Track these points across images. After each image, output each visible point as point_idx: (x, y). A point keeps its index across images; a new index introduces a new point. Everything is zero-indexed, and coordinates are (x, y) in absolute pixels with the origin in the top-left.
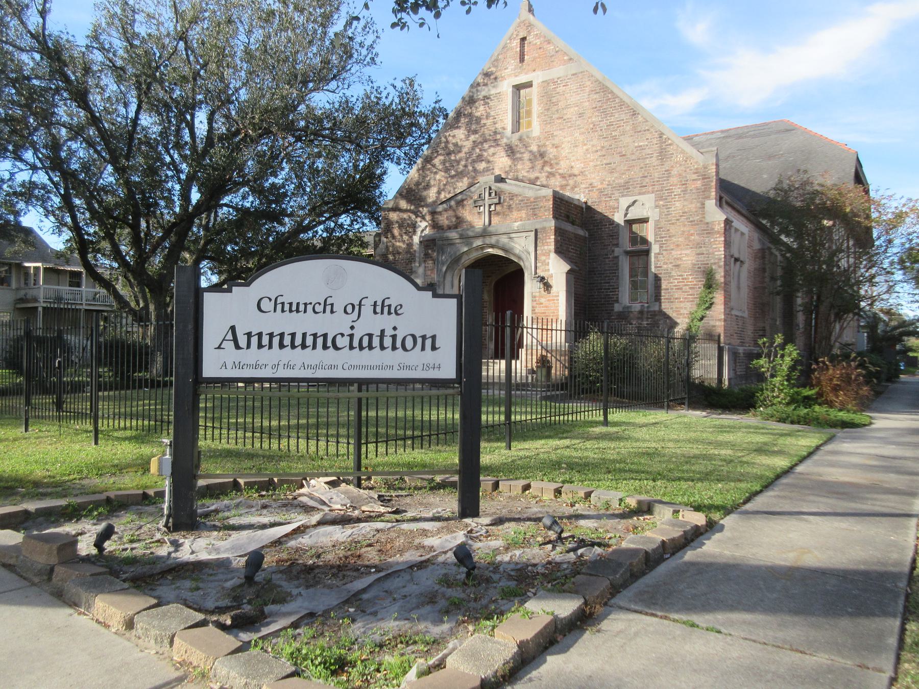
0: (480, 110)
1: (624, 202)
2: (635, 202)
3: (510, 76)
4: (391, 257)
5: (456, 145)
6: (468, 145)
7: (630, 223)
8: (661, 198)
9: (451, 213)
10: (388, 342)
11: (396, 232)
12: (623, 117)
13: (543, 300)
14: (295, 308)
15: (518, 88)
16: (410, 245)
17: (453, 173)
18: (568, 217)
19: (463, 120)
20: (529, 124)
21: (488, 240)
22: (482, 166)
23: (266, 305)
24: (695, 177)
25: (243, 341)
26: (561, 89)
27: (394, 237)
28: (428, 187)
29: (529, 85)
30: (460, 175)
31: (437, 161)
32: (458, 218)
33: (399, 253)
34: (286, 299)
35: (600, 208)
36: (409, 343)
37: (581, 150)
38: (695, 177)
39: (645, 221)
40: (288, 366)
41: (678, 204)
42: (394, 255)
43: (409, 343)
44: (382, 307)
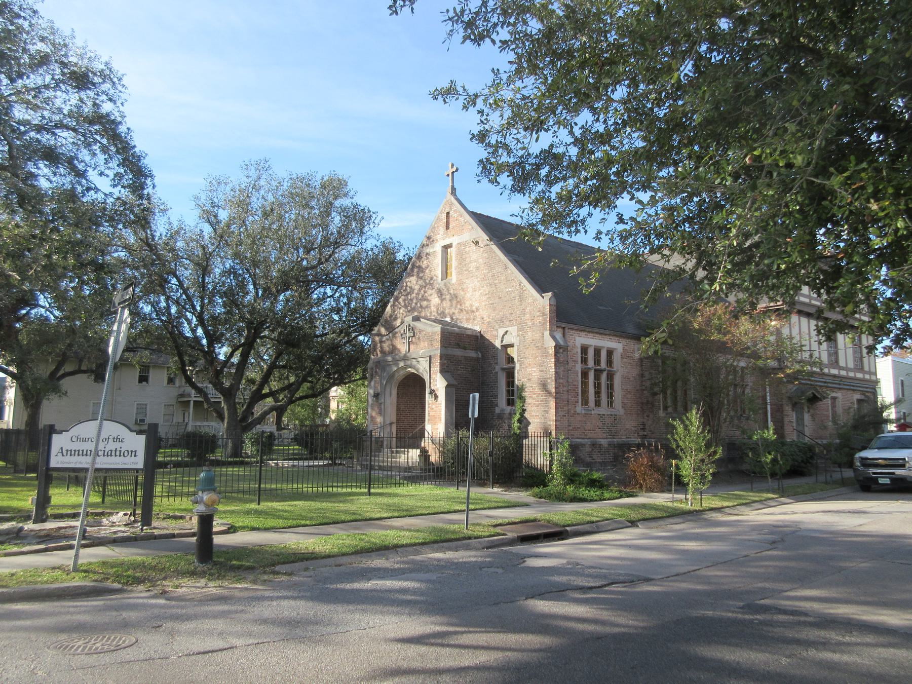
0: (424, 264)
1: (501, 332)
2: (506, 332)
5: (411, 288)
6: (417, 287)
7: (505, 347)
8: (520, 329)
9: (389, 342)
10: (118, 453)
12: (500, 270)
14: (84, 440)
15: (446, 248)
18: (458, 345)
19: (416, 270)
22: (425, 303)
23: (74, 439)
24: (538, 314)
25: (65, 453)
28: (396, 319)
29: (450, 246)
31: (401, 300)
32: (393, 346)
34: (81, 437)
35: (488, 336)
36: (126, 454)
37: (478, 293)
38: (538, 314)
39: (512, 346)
40: (80, 463)
41: (529, 334)
43: (126, 454)
44: (117, 439)
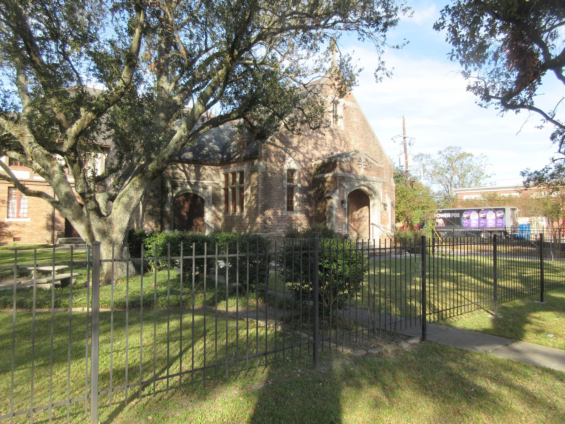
4: (269, 175)
11: (273, 159)
13: (384, 214)
16: (282, 170)
27: (271, 162)
32: (351, 167)
33: (275, 174)
42: (271, 174)
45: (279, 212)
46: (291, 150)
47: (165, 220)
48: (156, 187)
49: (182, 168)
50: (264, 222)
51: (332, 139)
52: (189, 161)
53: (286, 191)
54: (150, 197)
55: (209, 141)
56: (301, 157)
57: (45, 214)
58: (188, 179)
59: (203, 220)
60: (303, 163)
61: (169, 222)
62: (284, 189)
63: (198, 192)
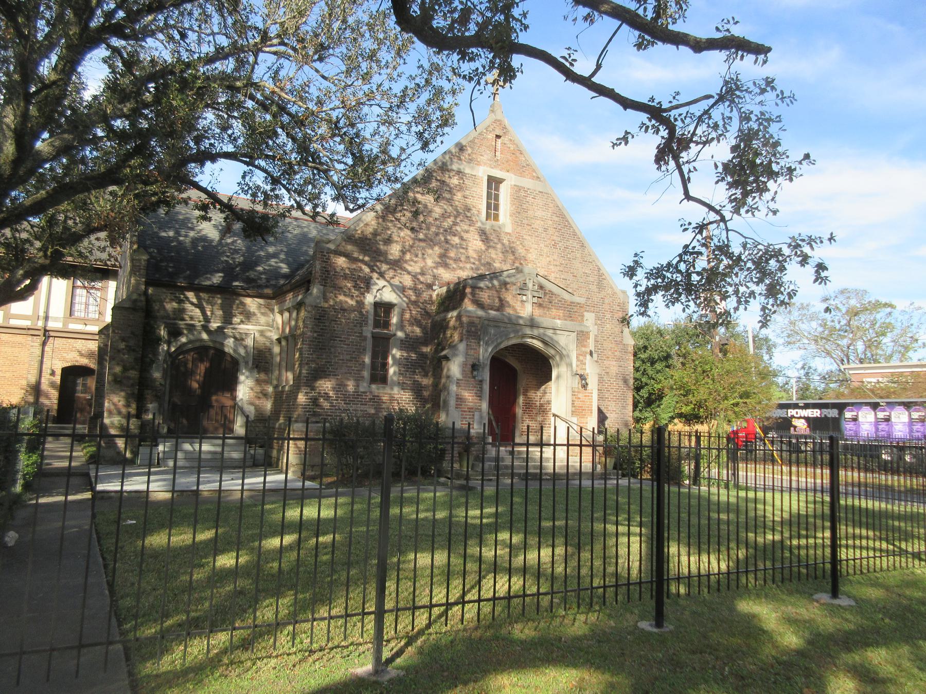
3: (485, 164)
8: (597, 318)
12: (575, 244)
13: (580, 395)
16: (361, 304)
17: (421, 236)
20: (496, 217)
21: (536, 332)
22: (456, 240)
24: (618, 308)
26: (529, 199)
28: (388, 241)
30: (430, 242)
32: (501, 300)
38: (618, 308)
45: (351, 386)
46: (384, 267)
47: (149, 394)
48: (133, 333)
49: (195, 301)
50: (315, 401)
51: (483, 248)
52: (213, 290)
53: (369, 344)
54: (119, 351)
55: (275, 256)
56: (407, 281)
57: (24, 383)
58: (207, 320)
59: (234, 398)
60: (411, 292)
61: (158, 398)
62: (365, 339)
63: (223, 344)
